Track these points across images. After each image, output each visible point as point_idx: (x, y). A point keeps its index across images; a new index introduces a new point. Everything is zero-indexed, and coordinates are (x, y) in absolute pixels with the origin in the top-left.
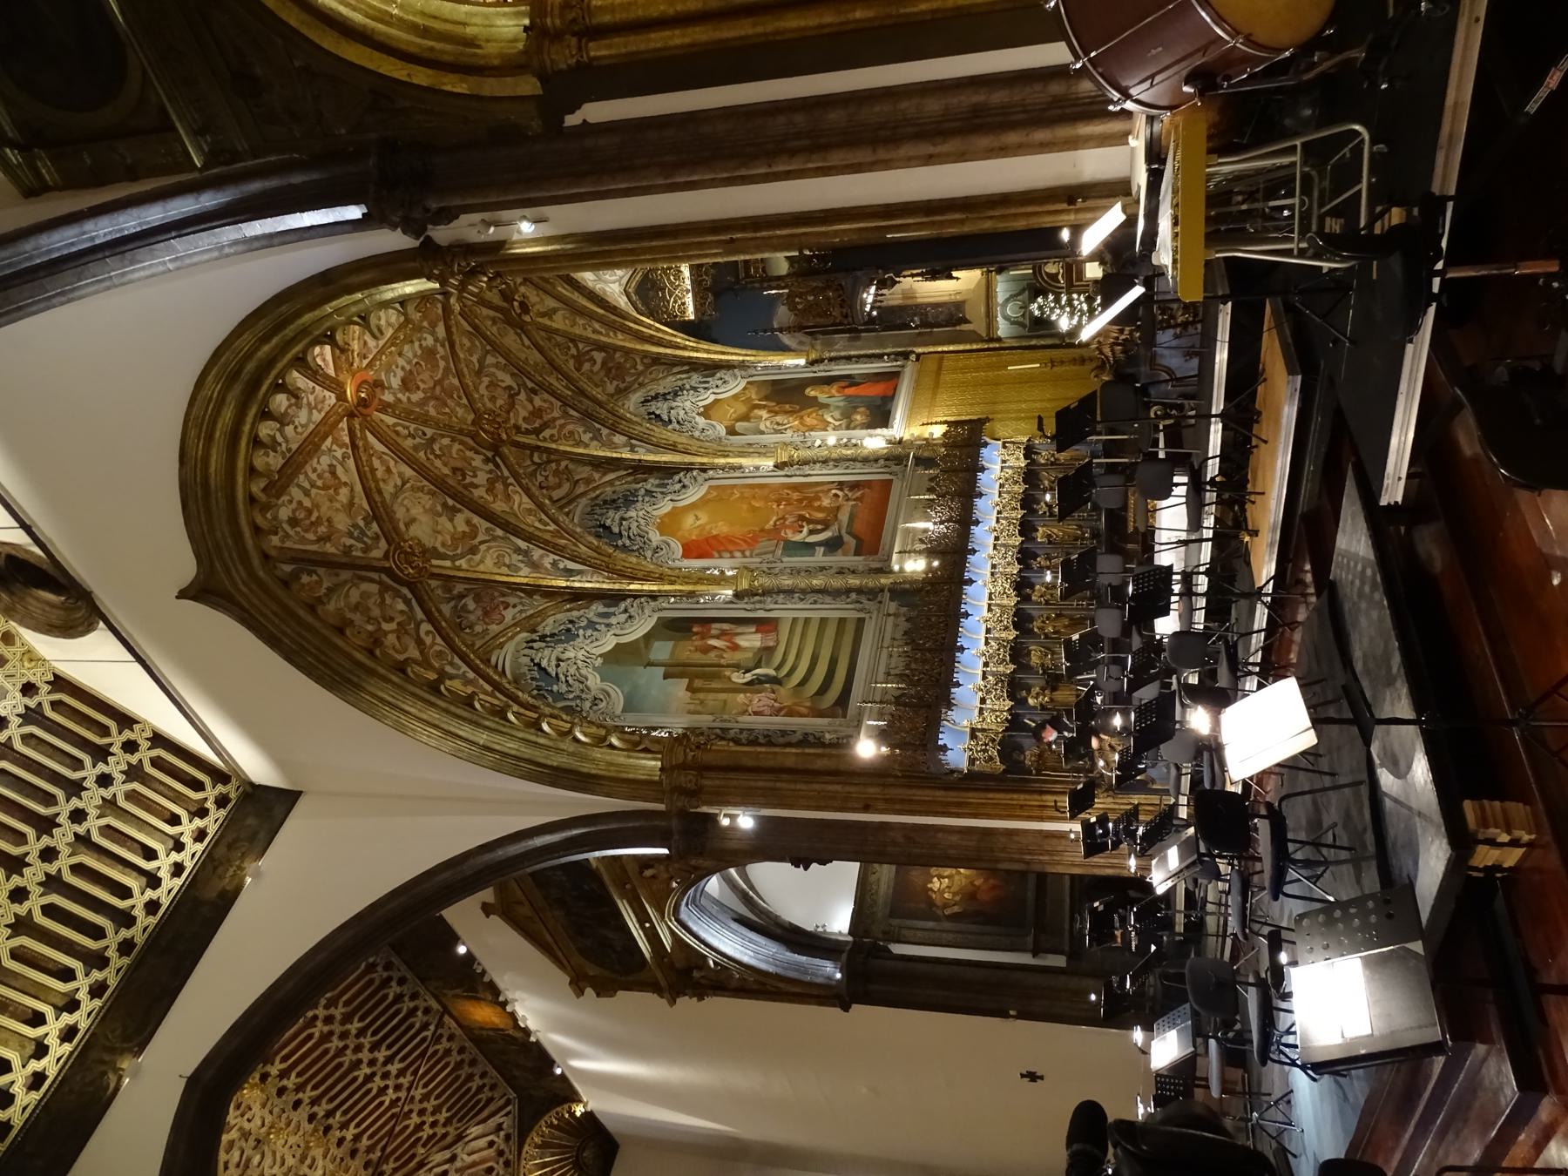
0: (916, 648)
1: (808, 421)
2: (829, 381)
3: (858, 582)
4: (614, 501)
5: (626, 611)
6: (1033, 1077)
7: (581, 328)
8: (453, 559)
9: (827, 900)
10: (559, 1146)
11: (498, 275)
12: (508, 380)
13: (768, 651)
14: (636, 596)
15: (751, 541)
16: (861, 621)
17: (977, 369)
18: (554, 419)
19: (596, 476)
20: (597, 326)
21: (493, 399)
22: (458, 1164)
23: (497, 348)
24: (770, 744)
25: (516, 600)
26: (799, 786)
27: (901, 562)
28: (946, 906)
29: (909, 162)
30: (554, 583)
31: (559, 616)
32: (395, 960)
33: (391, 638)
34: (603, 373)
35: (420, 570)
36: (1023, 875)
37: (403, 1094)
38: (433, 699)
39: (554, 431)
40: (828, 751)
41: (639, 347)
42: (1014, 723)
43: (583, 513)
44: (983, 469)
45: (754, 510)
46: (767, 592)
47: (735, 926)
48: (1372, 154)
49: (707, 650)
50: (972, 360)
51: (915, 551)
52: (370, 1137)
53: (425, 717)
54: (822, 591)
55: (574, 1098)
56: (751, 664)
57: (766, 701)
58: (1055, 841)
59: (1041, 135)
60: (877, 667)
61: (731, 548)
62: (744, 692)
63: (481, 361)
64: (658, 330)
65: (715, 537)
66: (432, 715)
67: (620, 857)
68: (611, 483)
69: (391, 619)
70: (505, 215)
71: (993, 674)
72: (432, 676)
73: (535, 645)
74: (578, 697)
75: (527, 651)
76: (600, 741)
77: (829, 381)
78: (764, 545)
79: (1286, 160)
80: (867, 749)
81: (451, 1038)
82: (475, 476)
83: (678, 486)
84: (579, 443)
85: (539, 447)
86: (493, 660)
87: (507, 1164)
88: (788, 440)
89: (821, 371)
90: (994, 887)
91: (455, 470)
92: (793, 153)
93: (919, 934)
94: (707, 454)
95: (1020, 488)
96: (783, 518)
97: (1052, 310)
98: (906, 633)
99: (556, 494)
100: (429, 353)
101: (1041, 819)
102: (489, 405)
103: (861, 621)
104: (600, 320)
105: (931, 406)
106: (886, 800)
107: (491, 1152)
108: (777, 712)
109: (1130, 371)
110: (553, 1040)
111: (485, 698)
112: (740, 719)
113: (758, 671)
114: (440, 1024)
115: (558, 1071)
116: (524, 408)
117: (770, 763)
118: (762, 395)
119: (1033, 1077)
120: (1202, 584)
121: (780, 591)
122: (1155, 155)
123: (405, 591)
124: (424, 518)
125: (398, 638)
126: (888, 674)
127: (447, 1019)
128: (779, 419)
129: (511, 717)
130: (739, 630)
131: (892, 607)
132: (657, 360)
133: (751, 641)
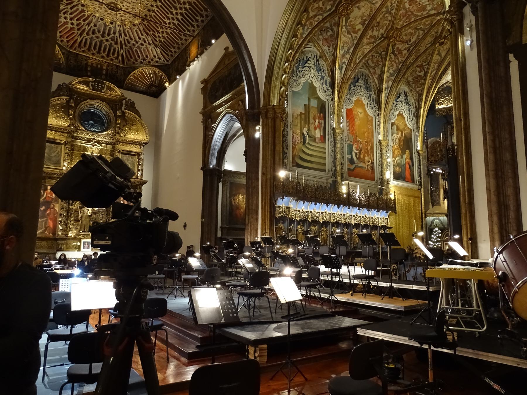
0: (316, 189)
1: (396, 152)
2: (411, 158)
3: (338, 169)
4: (367, 83)
5: (328, 90)
6: (185, 226)
7: (433, 66)
8: (346, 25)
9: (234, 162)
11: (451, 33)
12: (413, 40)
13: (314, 140)
14: (333, 93)
17: (415, 210)
18: (398, 59)
19: (377, 76)
20: (434, 72)
21: (406, 35)
22: (148, 46)
23: (425, 35)
24: (283, 142)
25: (331, 50)
26: (270, 151)
27: (345, 184)
28: (234, 200)
29: (488, 183)
30: (337, 63)
31: (325, 66)
32: (209, 18)
33: (316, 5)
34: (415, 76)
35: (341, 13)
36: (245, 224)
37: (168, 25)
38: (295, 23)
39: (393, 59)
41: (426, 88)
42: (292, 221)
44: (378, 211)
45: (364, 133)
46: (335, 139)
47: (225, 132)
50: (418, 208)
51: (349, 189)
52: (154, 16)
53: (289, 21)
54: (335, 158)
55: (170, 83)
56: (310, 134)
57: (297, 140)
58: (255, 233)
59: (496, 229)
60: (310, 177)
61: (350, 126)
62: (300, 132)
63: (421, 29)
64: (432, 95)
65: (354, 120)
66: (290, 23)
67: (245, 93)
68: (374, 81)
69: (323, 5)
70: (474, 34)
71: (308, 214)
72: (303, 22)
73: (315, 58)
75: (313, 56)
76: (282, 84)
77: (411, 158)
78: (352, 138)
79: (475, 305)
80: (282, 174)
81: (186, 40)
82: (376, 31)
83: (373, 106)
84: (389, 69)
85: (387, 54)
86: (310, 44)
87: (149, 62)
88: (389, 144)
89: (415, 155)
90: (241, 215)
91: (379, 23)
92: (493, 141)
93: (225, 191)
94: (384, 116)
95: (371, 224)
96: (361, 144)
97: (436, 235)
99: (370, 62)
100: (424, 8)
101: (262, 229)
102: (403, 34)
104: (436, 73)
105: (401, 194)
107: (152, 57)
108: (294, 144)
109: (409, 258)
110: (187, 74)
111: (296, 42)
112: (291, 131)
113: (307, 137)
114: (190, 36)
115: (178, 77)
116: (403, 47)
117: (277, 142)
118: (407, 135)
119: (185, 226)
120: (336, 279)
121: (335, 143)
122: (483, 265)
123: (334, 9)
124: (360, 13)
125: (317, 8)
126: (307, 180)
127: (192, 38)
128: (397, 141)
129: (290, 52)
130: (322, 130)
131: (330, 181)
132: (421, 95)
133: (318, 134)
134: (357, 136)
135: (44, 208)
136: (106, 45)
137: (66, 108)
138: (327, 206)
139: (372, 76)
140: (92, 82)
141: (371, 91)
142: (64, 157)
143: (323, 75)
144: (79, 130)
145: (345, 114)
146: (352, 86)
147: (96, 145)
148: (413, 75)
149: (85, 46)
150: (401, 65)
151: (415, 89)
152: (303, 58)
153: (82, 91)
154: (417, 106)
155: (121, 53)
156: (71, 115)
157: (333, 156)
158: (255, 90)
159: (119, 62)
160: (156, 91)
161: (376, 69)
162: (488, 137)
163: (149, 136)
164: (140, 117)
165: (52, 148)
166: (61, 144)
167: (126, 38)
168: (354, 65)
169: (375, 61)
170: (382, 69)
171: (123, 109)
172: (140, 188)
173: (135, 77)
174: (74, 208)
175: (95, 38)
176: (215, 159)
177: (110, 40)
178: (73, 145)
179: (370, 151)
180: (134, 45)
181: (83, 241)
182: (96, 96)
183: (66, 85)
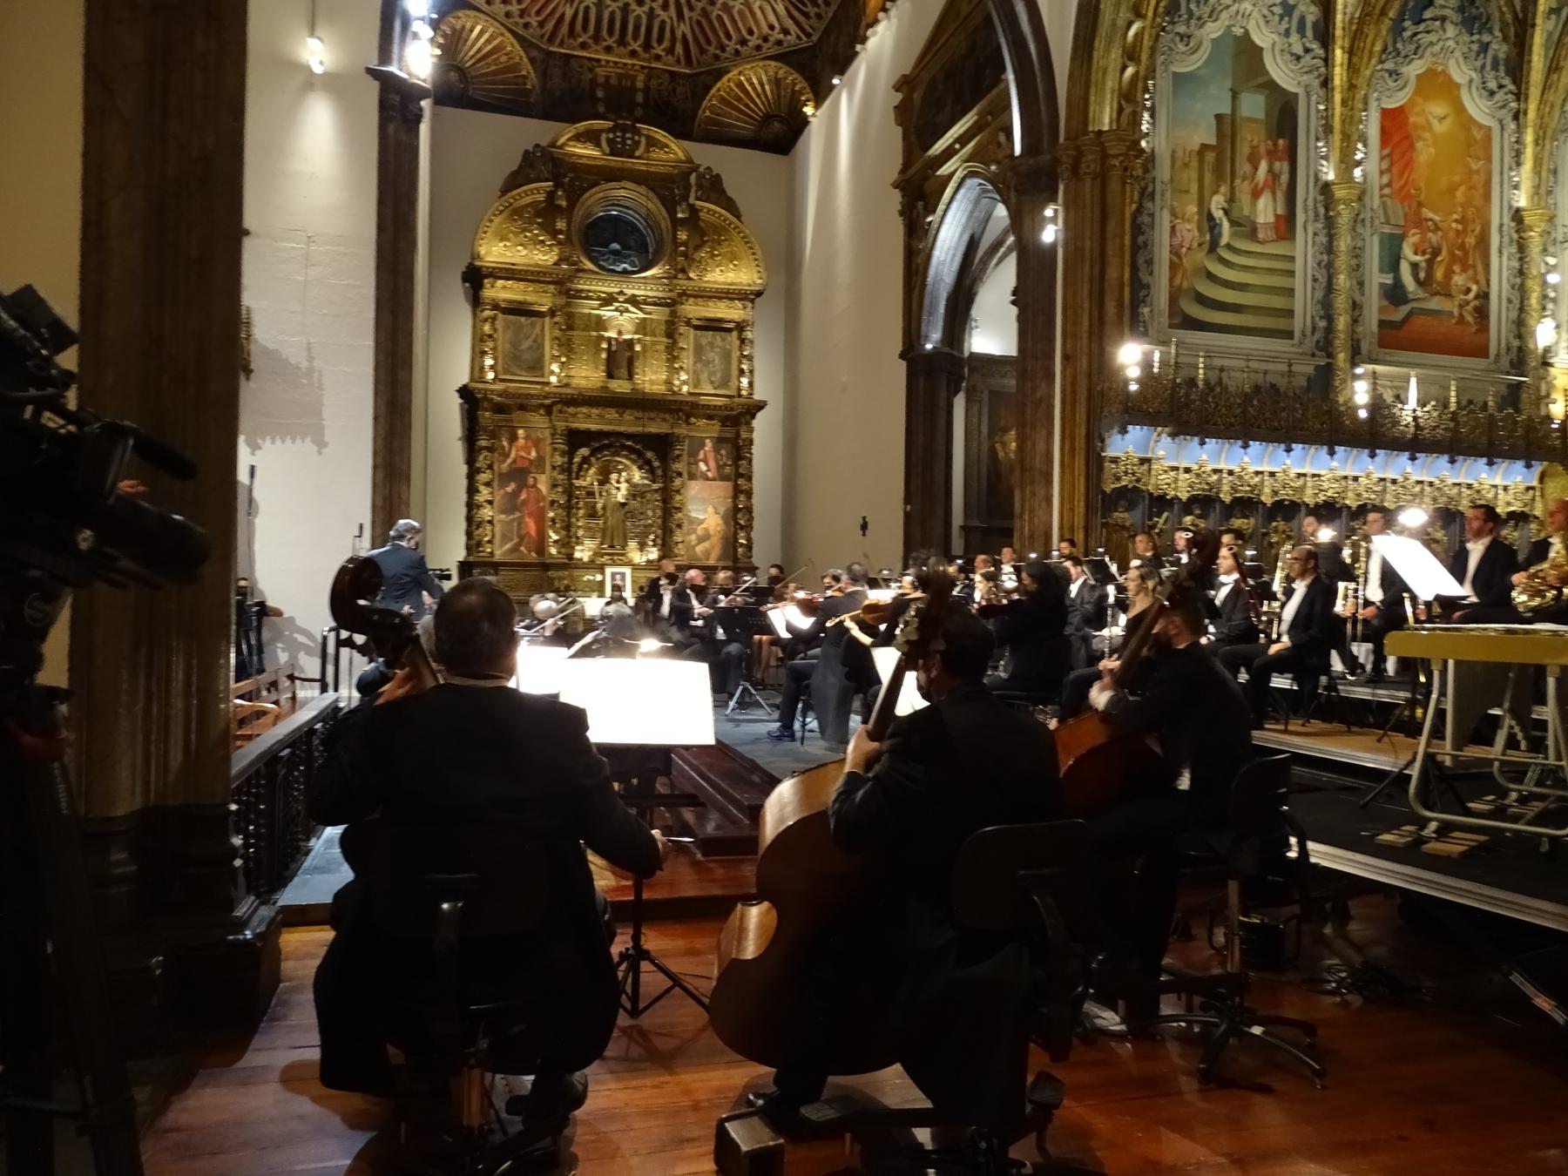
0: (1247, 398)
5: (1307, 50)
6: (864, 527)
14: (1327, 61)
16: (1289, 335)
24: (1135, 249)
26: (1086, 286)
28: (1004, 445)
36: (1011, 516)
40: (1127, 312)
42: (1161, 502)
44: (1490, 464)
45: (1452, 189)
46: (1330, 223)
47: (966, 237)
49: (1254, 161)
54: (1330, 288)
56: (1235, 214)
57: (1188, 237)
62: (1200, 213)
65: (1412, 147)
71: (1220, 480)
74: (1190, 14)
76: (1131, 55)
78: (1398, 211)
83: (1492, 85)
87: (758, 48)
93: (975, 420)
94: (1541, 116)
96: (1437, 228)
98: (1273, 386)
103: (1289, 335)
106: (1074, 378)
107: (766, 30)
108: (1175, 252)
110: (860, 69)
113: (1226, 224)
115: (836, 81)
117: (1111, 249)
119: (864, 527)
121: (1331, 237)
126: (1222, 370)
130: (1280, 196)
131: (1306, 368)
133: (1265, 211)
136: (638, 17)
137: (545, 216)
140: (610, 130)
141: (1490, 31)
145: (1373, 129)
146: (1407, 24)
147: (627, 311)
149: (585, 28)
153: (584, 161)
155: (679, 35)
156: (561, 232)
157: (1323, 280)
160: (780, 133)
163: (766, 269)
164: (738, 217)
166: (540, 315)
171: (692, 200)
172: (748, 423)
173: (722, 100)
174: (584, 484)
176: (940, 324)
178: (570, 316)
179: (1475, 253)
181: (609, 571)
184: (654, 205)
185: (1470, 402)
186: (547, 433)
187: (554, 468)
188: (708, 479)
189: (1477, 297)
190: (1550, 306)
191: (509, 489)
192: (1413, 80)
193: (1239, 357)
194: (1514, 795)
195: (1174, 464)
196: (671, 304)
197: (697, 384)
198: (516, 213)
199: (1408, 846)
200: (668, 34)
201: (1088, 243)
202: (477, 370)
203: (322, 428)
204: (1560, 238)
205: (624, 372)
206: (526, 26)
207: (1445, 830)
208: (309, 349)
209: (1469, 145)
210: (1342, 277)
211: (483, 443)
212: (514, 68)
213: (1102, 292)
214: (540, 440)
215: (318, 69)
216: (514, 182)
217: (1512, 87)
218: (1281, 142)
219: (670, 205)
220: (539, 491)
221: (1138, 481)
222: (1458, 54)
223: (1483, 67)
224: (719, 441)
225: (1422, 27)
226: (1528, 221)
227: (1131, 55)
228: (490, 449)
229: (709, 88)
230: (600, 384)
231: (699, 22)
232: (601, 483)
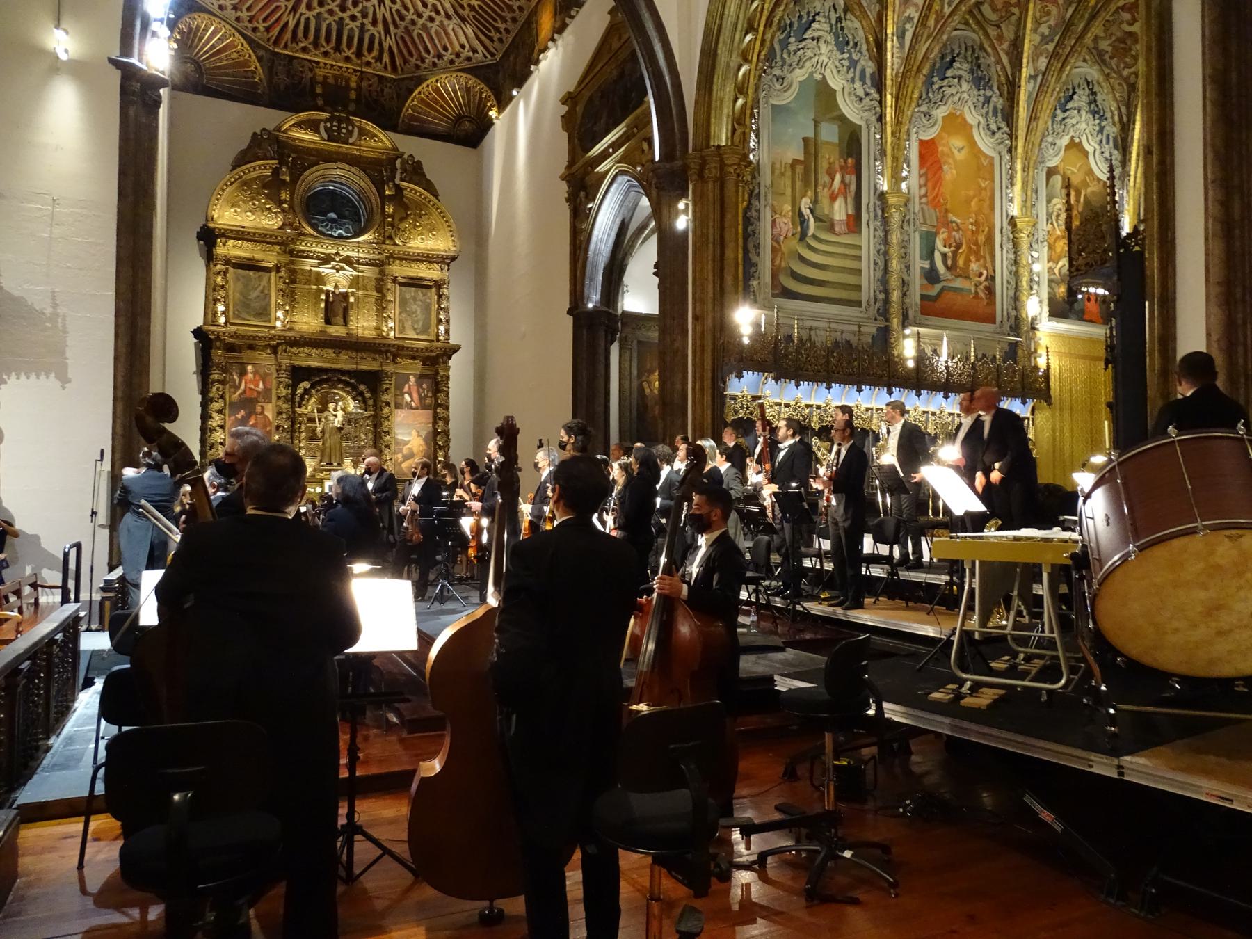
0: (829, 351)
4: (979, 66)
5: (867, 94)
9: (640, 297)
10: (469, 101)
13: (831, 227)
14: (881, 102)
15: (935, 202)
19: (1005, 46)
22: (446, 22)
24: (746, 237)
28: (649, 383)
30: (890, 21)
31: (861, 32)
34: (1119, 34)
40: (741, 283)
43: (966, 37)
45: (968, 201)
46: (885, 221)
47: (618, 221)
48: (1041, 689)
55: (501, 109)
56: (818, 213)
57: (785, 229)
62: (793, 210)
65: (941, 168)
67: (650, 122)
68: (999, 61)
71: (811, 413)
74: (784, 61)
76: (741, 90)
78: (932, 215)
83: (994, 127)
84: (1037, 23)
87: (452, 62)
93: (627, 364)
96: (959, 229)
103: (858, 304)
105: (1070, 355)
107: (458, 48)
108: (775, 239)
110: (534, 84)
113: (812, 220)
115: (515, 93)
117: (728, 236)
121: (886, 232)
126: (811, 329)
130: (850, 200)
133: (840, 211)
134: (947, 211)
135: (242, 413)
136: (352, 29)
137: (271, 188)
138: (860, 390)
139: (994, 48)
140: (327, 120)
141: (991, 88)
142: (277, 298)
143: (855, 57)
144: (304, 235)
146: (935, 79)
147: (343, 269)
148: (1112, 34)
149: (306, 36)
150: (1071, 10)
151: (1119, 73)
152: (800, 17)
153: (305, 144)
154: (1125, 119)
155: (386, 46)
156: (285, 202)
158: (674, 112)
159: (385, 67)
160: (470, 132)
161: (1003, 26)
162: (1211, 193)
164: (436, 196)
165: (249, 279)
166: (268, 270)
167: (395, 7)
168: (937, 22)
169: (1000, 6)
170: (1019, 24)
171: (397, 181)
172: (445, 363)
173: (422, 101)
174: (306, 411)
175: (326, 15)
177: (359, 15)
179: (983, 247)
180: (413, 22)
182: (337, 153)
183: (269, 133)
184: (365, 183)
185: (984, 355)
186: (273, 369)
187: (279, 398)
188: (412, 408)
189: (986, 279)
190: (1035, 287)
191: (239, 416)
192: (940, 120)
193: (823, 320)
194: (1022, 656)
195: (778, 400)
196: (380, 265)
197: (402, 330)
198: (246, 184)
199: (952, 701)
200: (376, 45)
201: (711, 231)
202: (210, 314)
203: (65, 366)
204: (1041, 239)
205: (340, 319)
206: (255, 30)
207: (976, 687)
208: (53, 298)
209: (979, 170)
210: (894, 262)
211: (216, 377)
212: (246, 63)
213: (722, 269)
214: (266, 374)
215: (63, 57)
216: (243, 159)
217: (1006, 129)
218: (850, 160)
219: (379, 185)
220: (266, 417)
221: (751, 413)
222: (970, 103)
223: (987, 113)
224: (421, 377)
225: (945, 82)
226: (1019, 226)
227: (741, 90)
228: (222, 382)
229: (411, 92)
230: (319, 329)
231: (402, 38)
232: (320, 411)
